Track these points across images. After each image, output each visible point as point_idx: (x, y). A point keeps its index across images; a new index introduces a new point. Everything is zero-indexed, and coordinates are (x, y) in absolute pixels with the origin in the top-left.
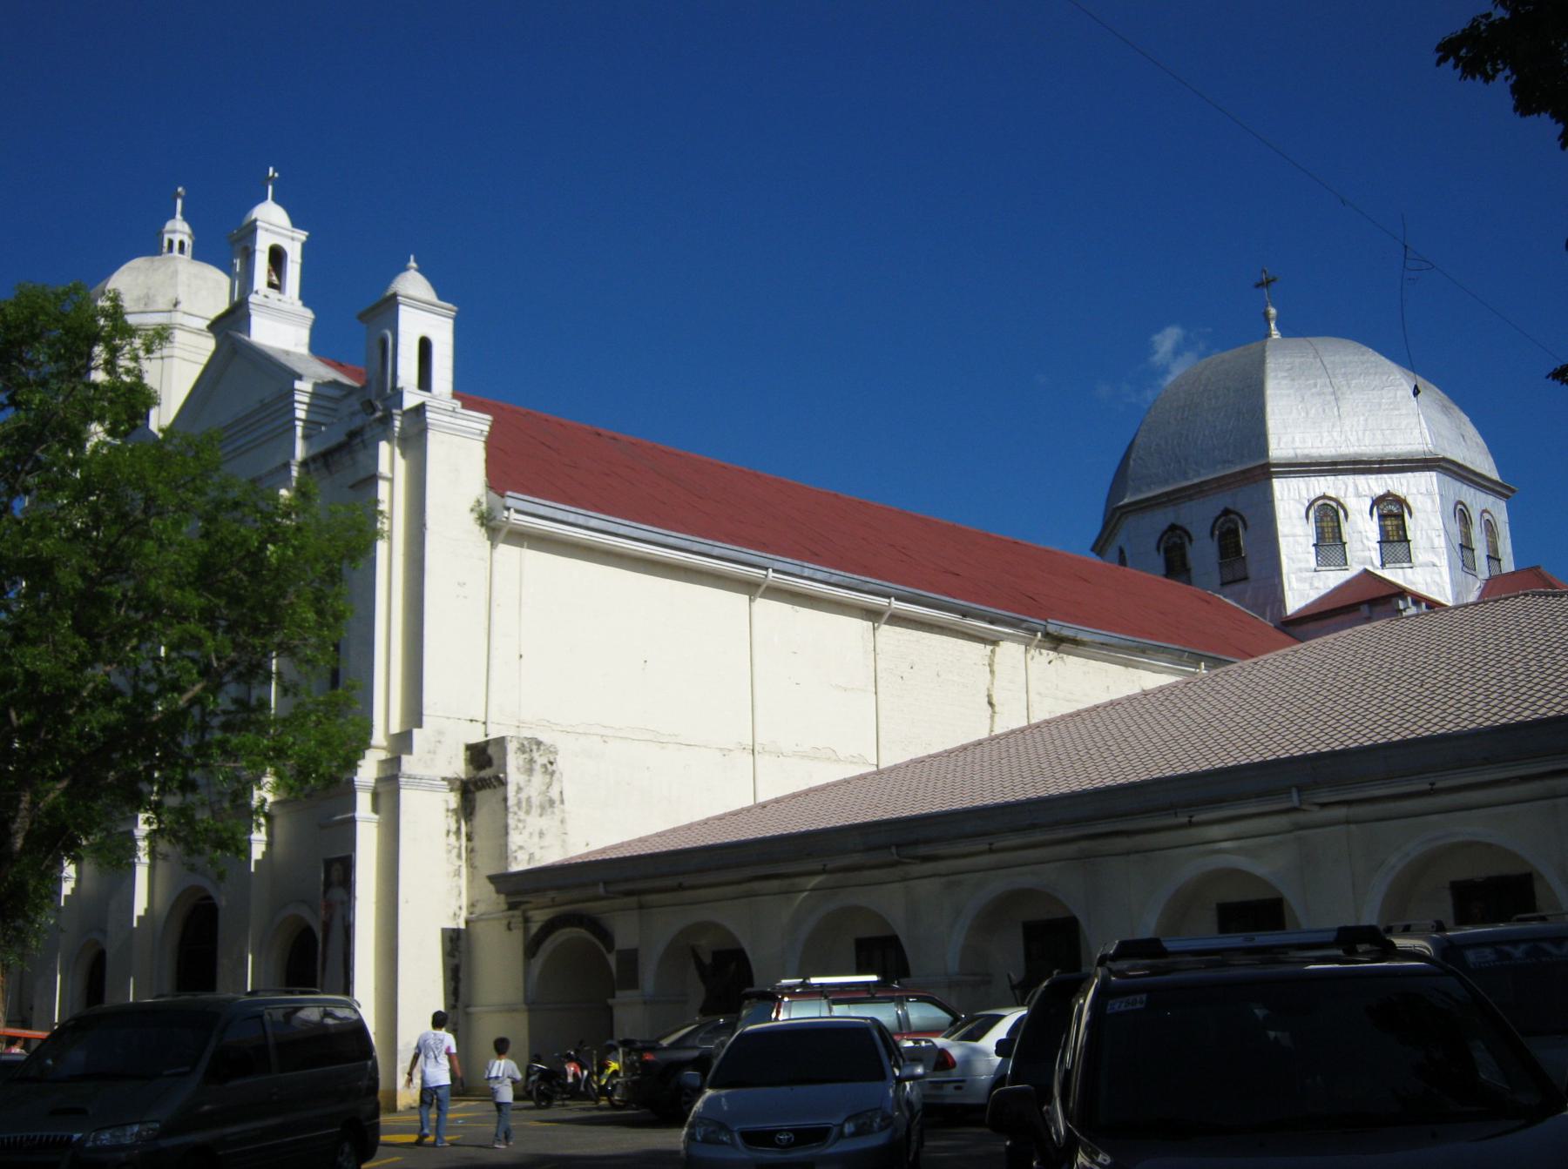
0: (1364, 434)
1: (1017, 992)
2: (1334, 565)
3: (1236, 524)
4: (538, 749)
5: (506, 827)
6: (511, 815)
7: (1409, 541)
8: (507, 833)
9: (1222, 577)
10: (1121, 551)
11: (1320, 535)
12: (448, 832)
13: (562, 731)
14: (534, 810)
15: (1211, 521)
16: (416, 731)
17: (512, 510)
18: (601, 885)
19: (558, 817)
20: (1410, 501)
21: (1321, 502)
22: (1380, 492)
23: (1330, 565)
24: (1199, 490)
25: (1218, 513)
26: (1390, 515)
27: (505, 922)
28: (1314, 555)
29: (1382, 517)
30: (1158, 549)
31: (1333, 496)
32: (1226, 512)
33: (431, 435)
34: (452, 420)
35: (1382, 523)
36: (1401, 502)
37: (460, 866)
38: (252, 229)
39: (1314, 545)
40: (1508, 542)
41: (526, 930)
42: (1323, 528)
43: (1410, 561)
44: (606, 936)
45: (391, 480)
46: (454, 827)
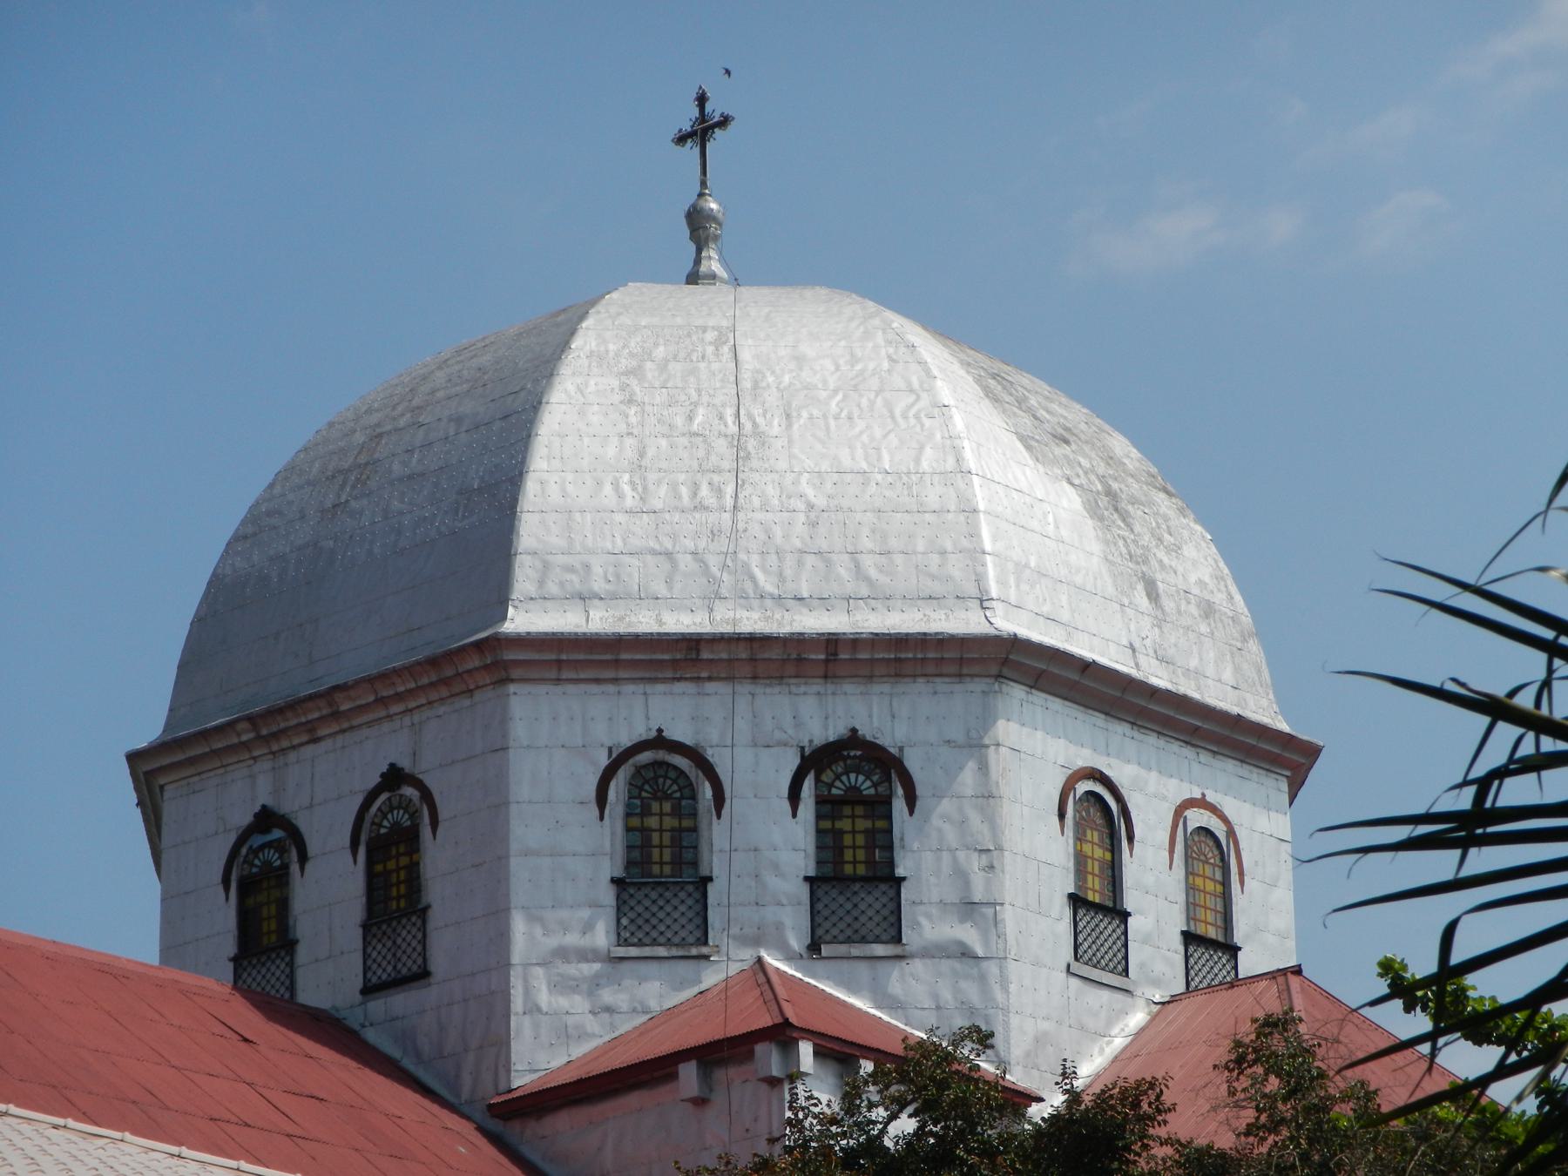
0: (800, 563)
2: (668, 943)
3: (414, 815)
9: (366, 969)
11: (636, 854)
15: (358, 801)
20: (913, 763)
21: (645, 757)
22: (835, 731)
23: (655, 943)
25: (374, 780)
26: (853, 798)
28: (612, 912)
29: (828, 807)
30: (226, 882)
31: (688, 741)
35: (827, 824)
39: (614, 881)
40: (1283, 896)
42: (645, 831)
43: (897, 939)
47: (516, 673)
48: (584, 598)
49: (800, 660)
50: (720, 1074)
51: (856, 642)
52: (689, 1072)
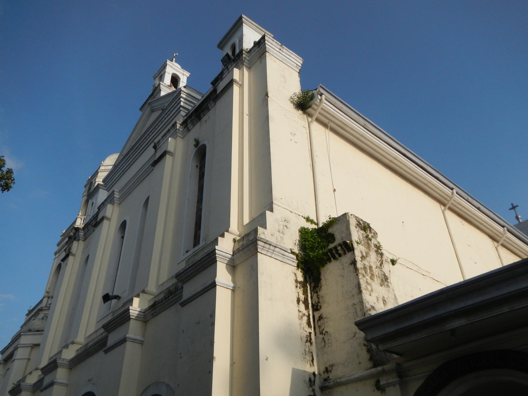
4: (370, 231)
5: (359, 286)
6: (360, 276)
8: (360, 292)
12: (298, 301)
14: (375, 279)
16: (268, 213)
17: (323, 96)
27: (373, 382)
33: (267, 54)
34: (281, 52)
37: (310, 333)
38: (165, 66)
45: (241, 86)
46: (302, 297)
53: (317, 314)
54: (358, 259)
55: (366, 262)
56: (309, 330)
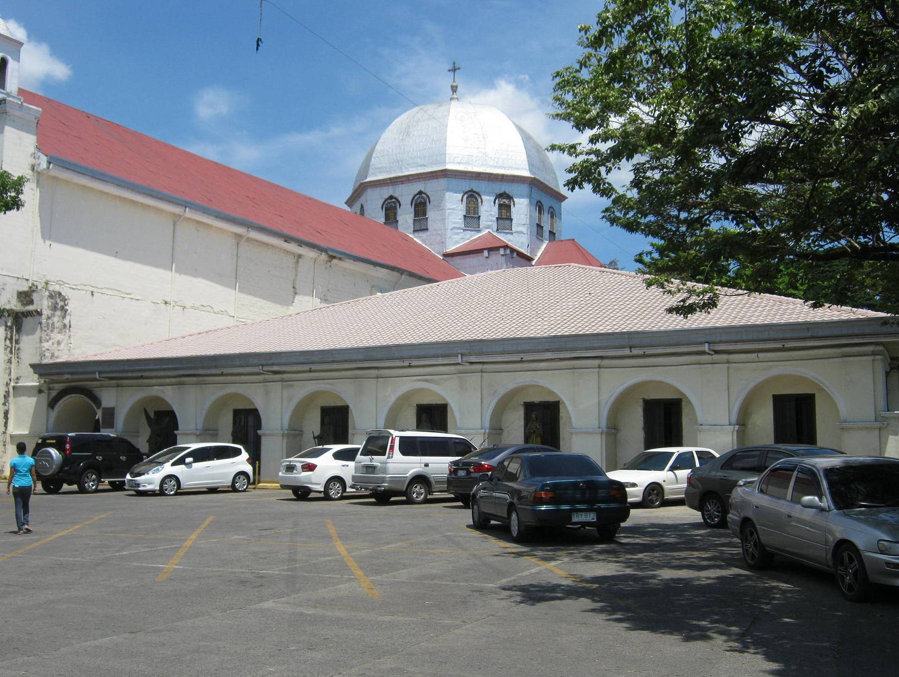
1: (316, 440)
7: (511, 220)
10: (362, 207)
13: (70, 288)
15: (412, 197)
18: (97, 373)
19: (67, 335)
21: (470, 193)
22: (502, 191)
24: (408, 179)
25: (416, 192)
29: (500, 206)
30: (382, 208)
32: (420, 193)
36: (510, 198)
37: (11, 357)
41: (49, 394)
44: (97, 401)
47: (448, 176)
48: (459, 163)
49: (497, 178)
50: (491, 252)
51: (507, 176)
52: (486, 253)
53: (17, 346)
54: (44, 321)
55: (50, 322)
56: (10, 356)
